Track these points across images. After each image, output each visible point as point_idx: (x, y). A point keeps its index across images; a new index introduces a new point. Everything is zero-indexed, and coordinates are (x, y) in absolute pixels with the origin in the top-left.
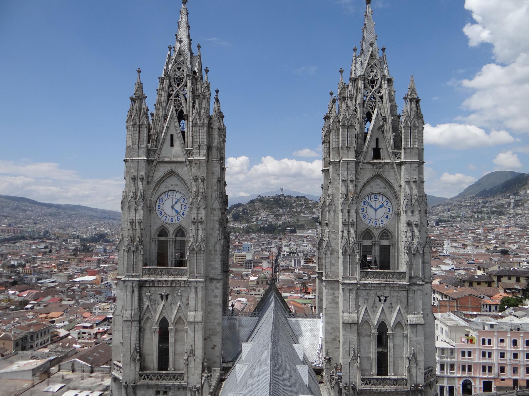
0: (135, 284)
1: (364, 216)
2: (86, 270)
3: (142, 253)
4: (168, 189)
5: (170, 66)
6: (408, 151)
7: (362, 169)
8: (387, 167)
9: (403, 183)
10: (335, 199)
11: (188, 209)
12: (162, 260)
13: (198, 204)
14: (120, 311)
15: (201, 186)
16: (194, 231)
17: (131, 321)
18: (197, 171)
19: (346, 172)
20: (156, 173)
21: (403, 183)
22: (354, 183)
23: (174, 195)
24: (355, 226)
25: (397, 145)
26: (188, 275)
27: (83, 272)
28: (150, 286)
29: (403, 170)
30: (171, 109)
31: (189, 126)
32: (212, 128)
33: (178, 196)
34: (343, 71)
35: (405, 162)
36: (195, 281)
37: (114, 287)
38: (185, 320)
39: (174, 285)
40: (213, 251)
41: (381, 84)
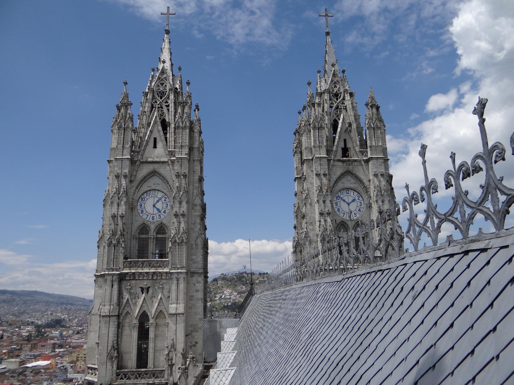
0: (115, 277)
1: (339, 210)
2: (39, 356)
3: (123, 245)
4: (150, 189)
5: (153, 84)
6: (373, 148)
7: (333, 166)
8: (356, 164)
9: (371, 177)
10: (311, 193)
11: (169, 207)
12: (142, 252)
13: (180, 198)
14: (97, 310)
15: (183, 181)
16: (176, 224)
17: (110, 316)
18: (180, 168)
19: (319, 167)
20: (139, 172)
21: (371, 177)
22: (328, 176)
23: (156, 194)
24: (331, 215)
25: (363, 144)
26: (170, 267)
27: (36, 358)
28: (130, 280)
29: (370, 167)
30: (155, 115)
31: (171, 132)
32: (193, 131)
33: (160, 195)
34: (310, 83)
35: (372, 158)
36: (177, 272)
37: (70, 370)
38: (166, 313)
39: (155, 278)
40: (194, 246)
41: (344, 97)
